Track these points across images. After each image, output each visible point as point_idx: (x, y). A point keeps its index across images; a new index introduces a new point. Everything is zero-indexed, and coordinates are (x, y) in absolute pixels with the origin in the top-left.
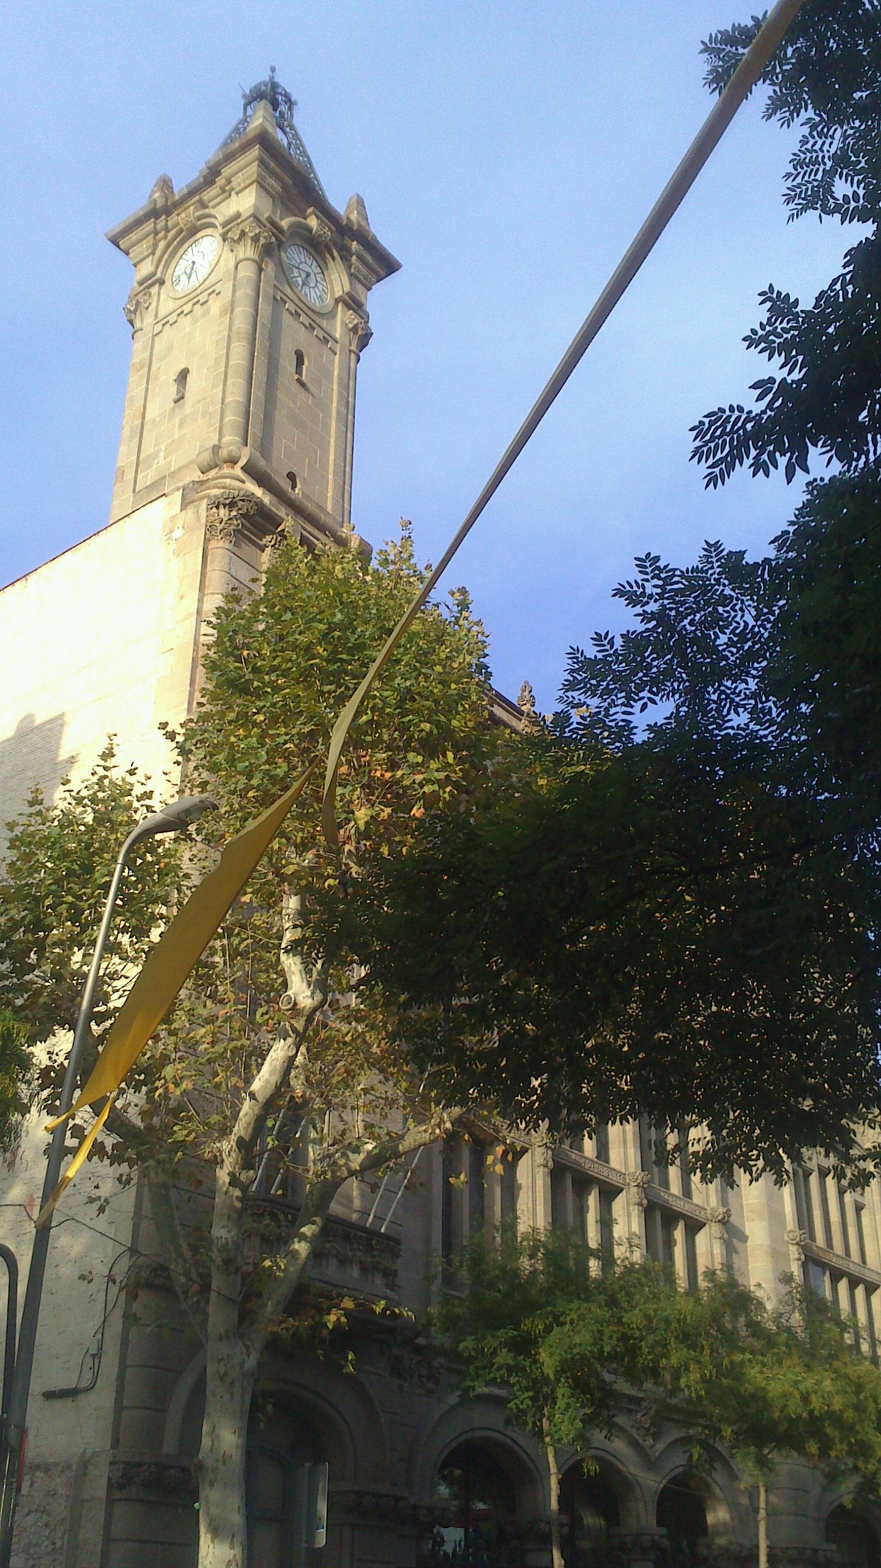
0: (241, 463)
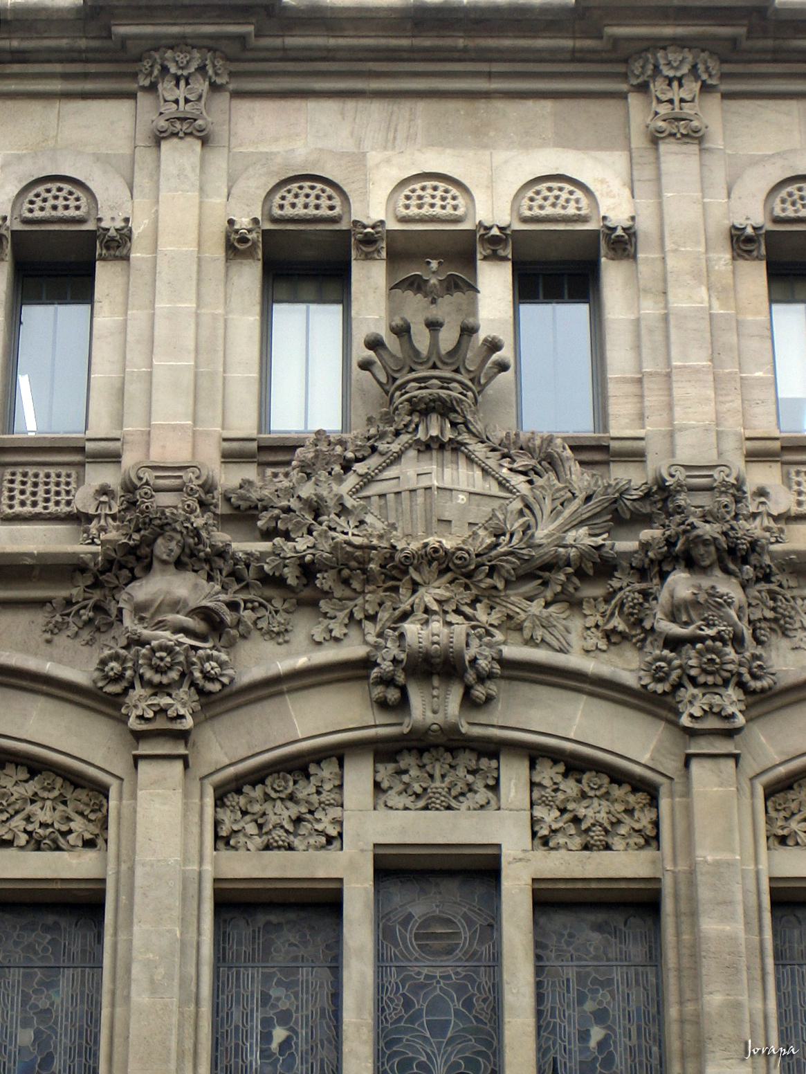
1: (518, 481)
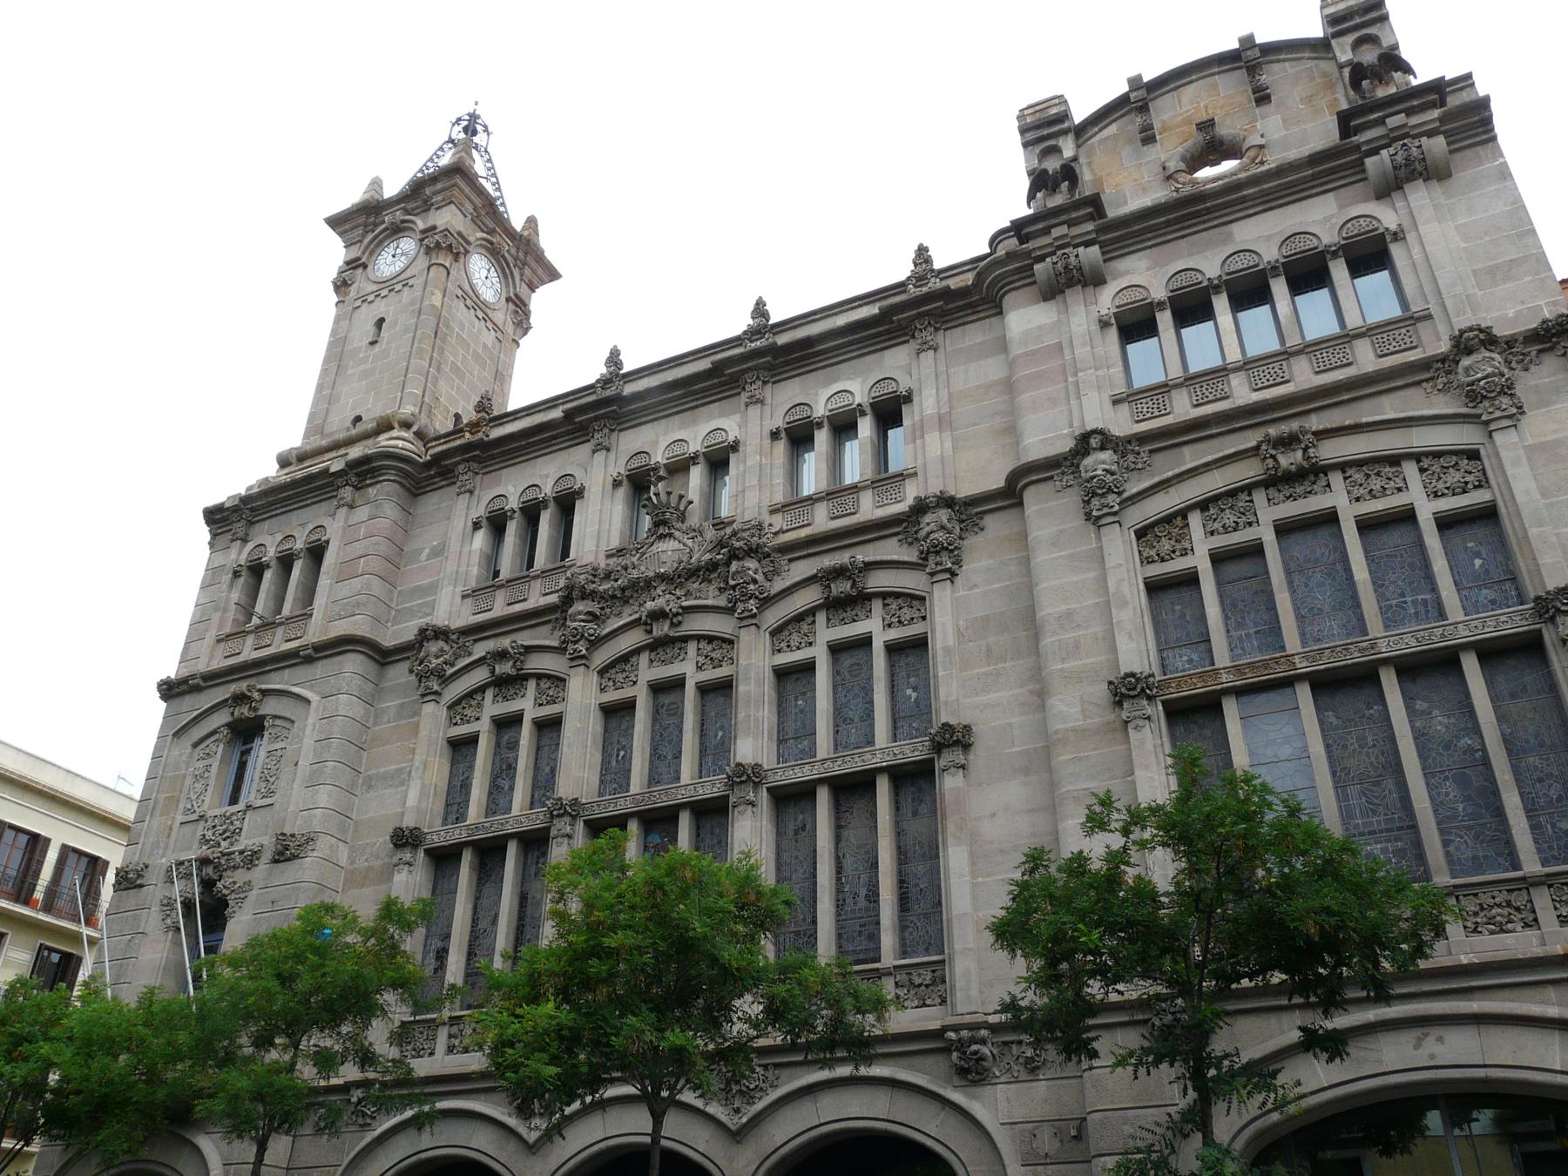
0: (415, 428)
1: (690, 543)
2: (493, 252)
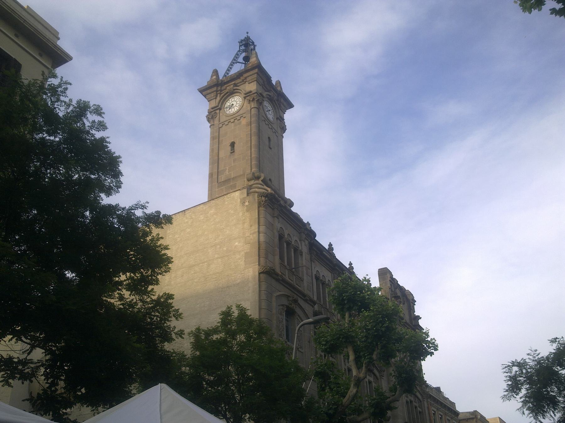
0: (262, 178)
2: (271, 100)
